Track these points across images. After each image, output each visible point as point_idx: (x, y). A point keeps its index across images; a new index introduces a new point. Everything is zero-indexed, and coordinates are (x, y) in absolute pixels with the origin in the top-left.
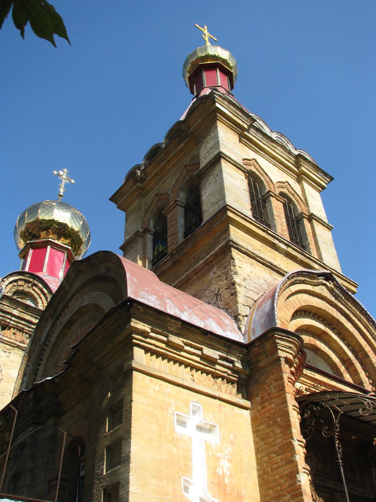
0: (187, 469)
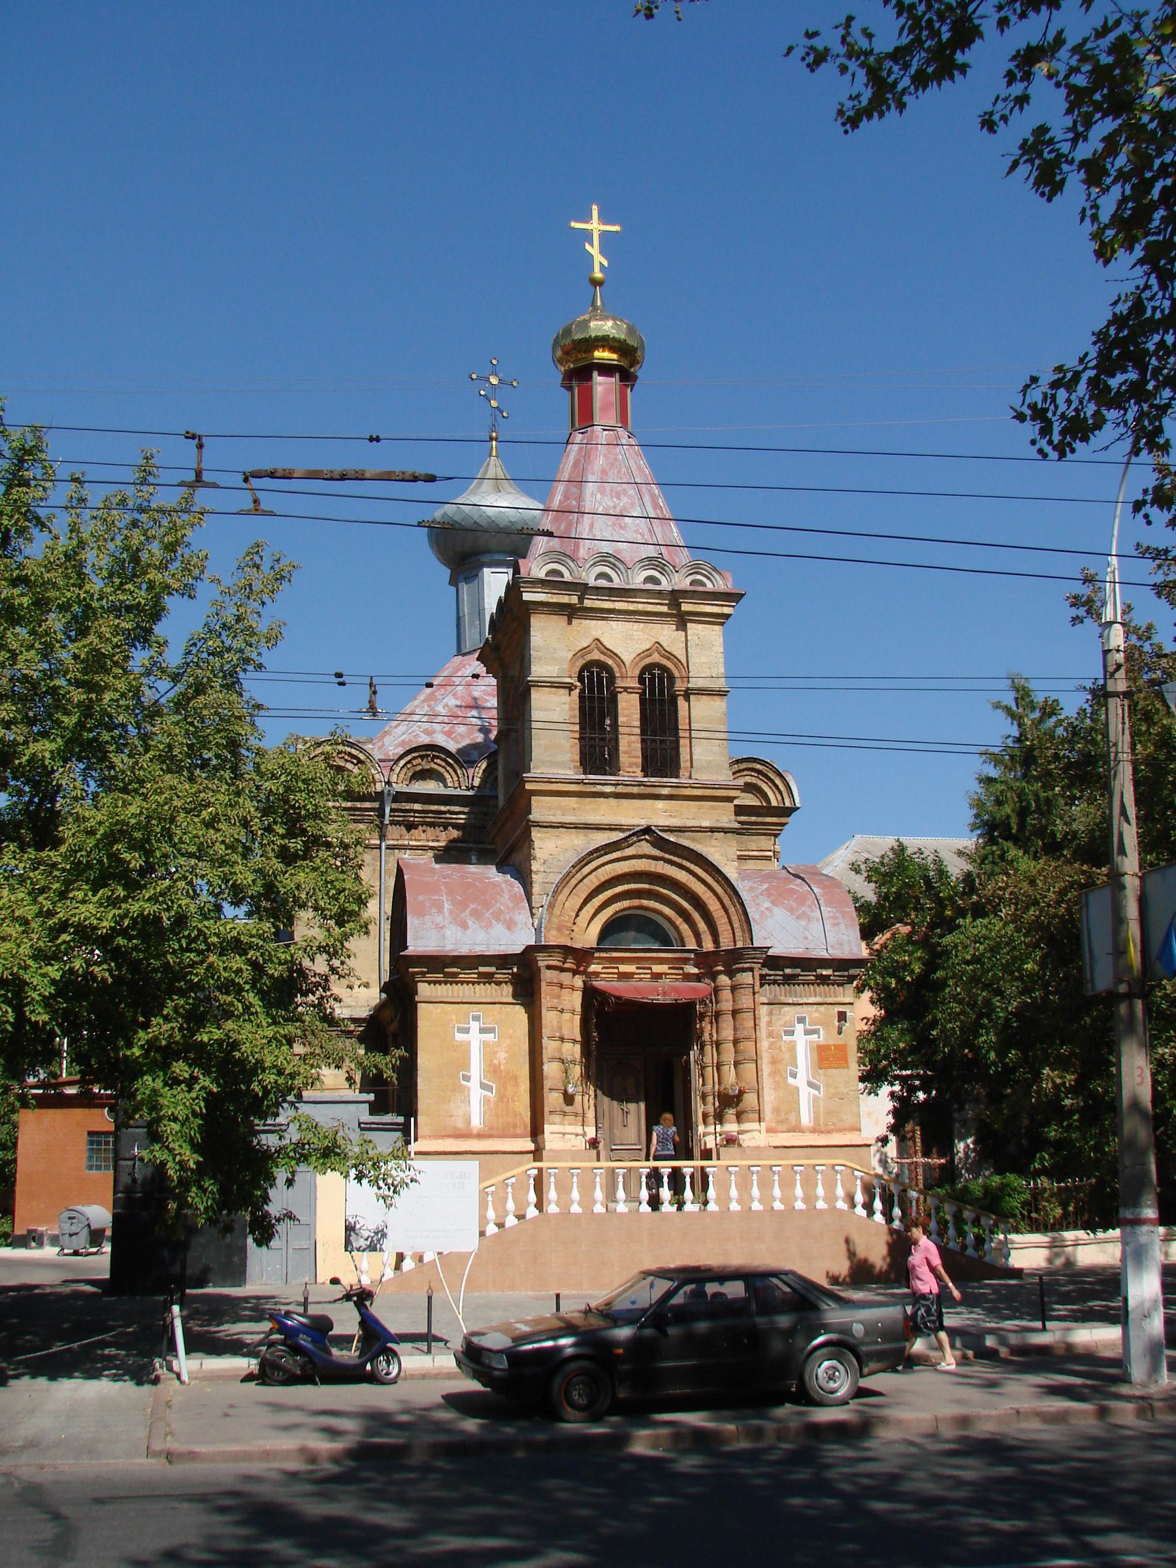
0: (466, 1065)
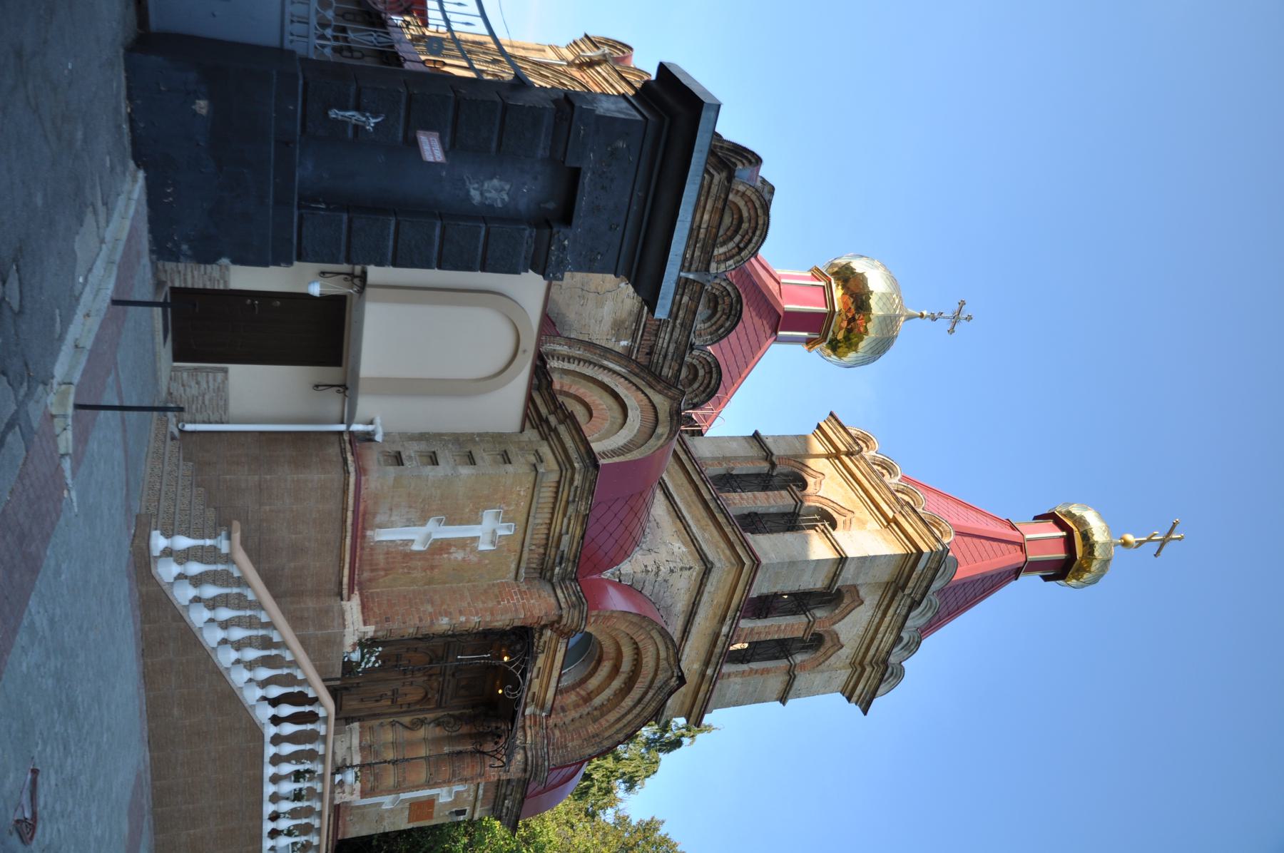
0: (450, 522)
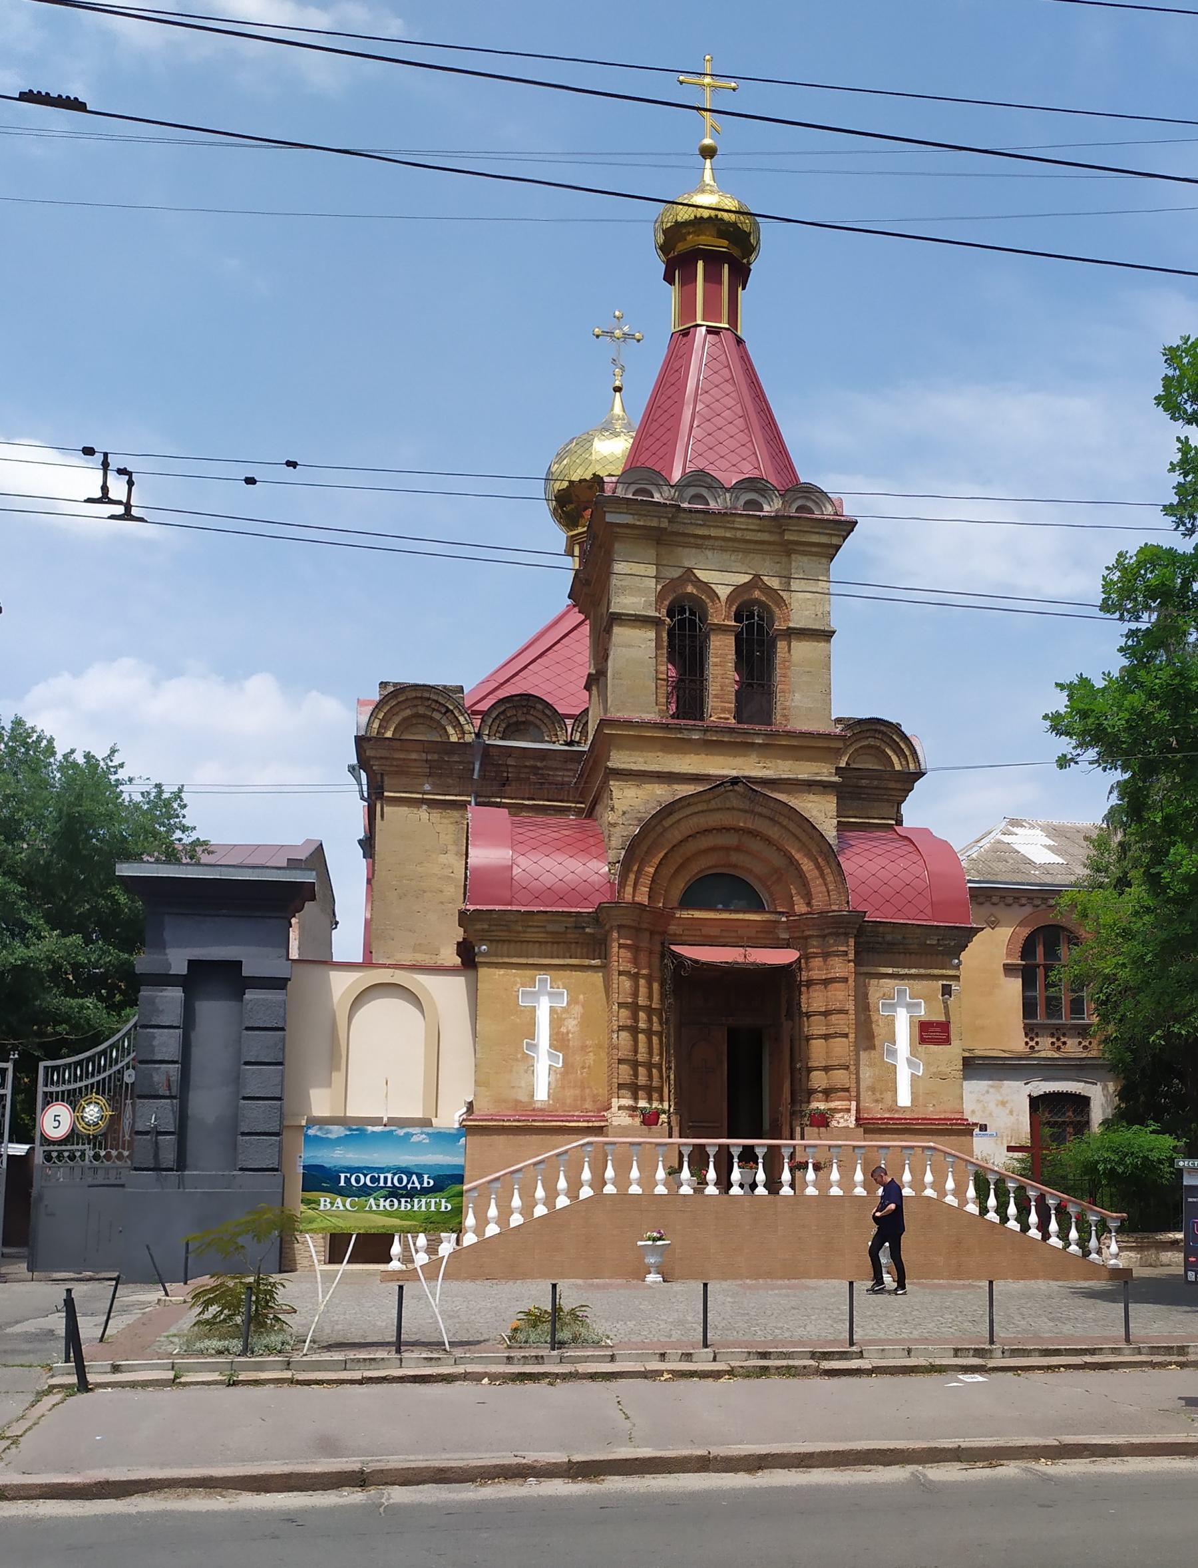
0: (532, 1035)
